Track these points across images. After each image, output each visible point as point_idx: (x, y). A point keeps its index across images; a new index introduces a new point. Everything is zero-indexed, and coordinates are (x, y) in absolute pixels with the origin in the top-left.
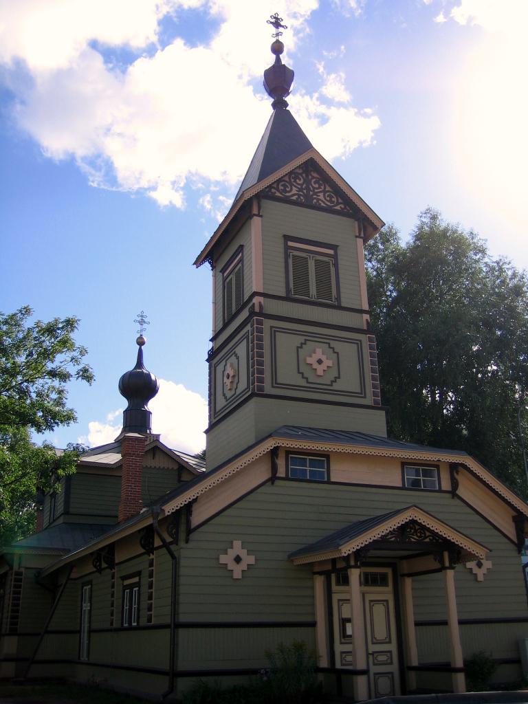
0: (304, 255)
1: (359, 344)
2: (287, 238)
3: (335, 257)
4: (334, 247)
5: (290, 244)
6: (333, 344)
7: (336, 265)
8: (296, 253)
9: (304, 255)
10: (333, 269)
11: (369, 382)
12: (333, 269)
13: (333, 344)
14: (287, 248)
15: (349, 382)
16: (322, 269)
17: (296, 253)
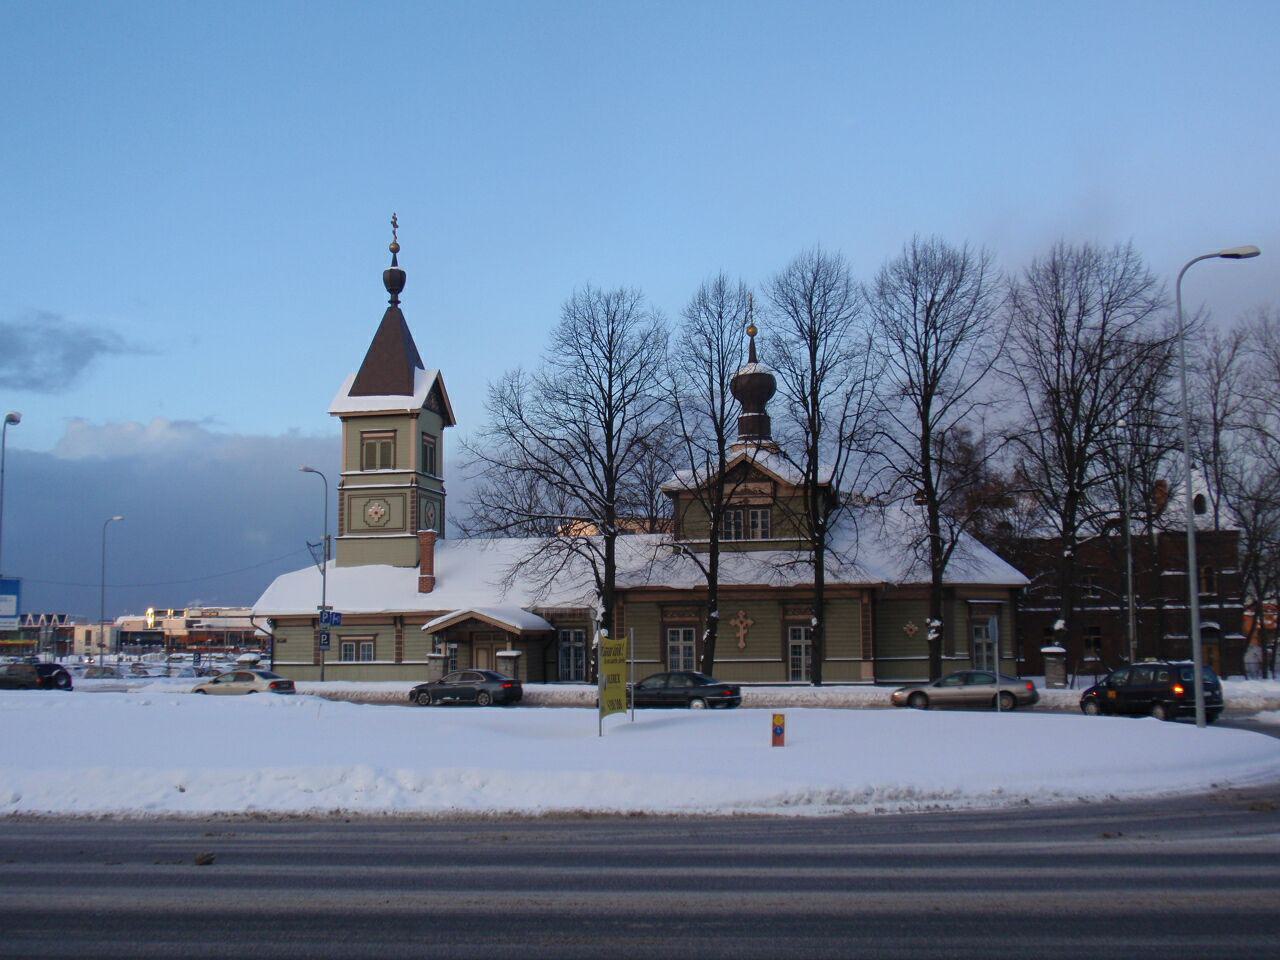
0: (373, 441)
1: (404, 495)
2: (363, 433)
3: (394, 438)
4: (395, 431)
5: (365, 435)
6: (387, 499)
7: (395, 444)
8: (369, 441)
9: (373, 441)
10: (392, 446)
11: (409, 520)
12: (392, 446)
13: (387, 499)
14: (362, 439)
15: (396, 522)
16: (385, 447)
17: (369, 441)
